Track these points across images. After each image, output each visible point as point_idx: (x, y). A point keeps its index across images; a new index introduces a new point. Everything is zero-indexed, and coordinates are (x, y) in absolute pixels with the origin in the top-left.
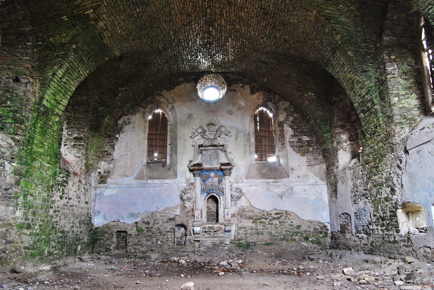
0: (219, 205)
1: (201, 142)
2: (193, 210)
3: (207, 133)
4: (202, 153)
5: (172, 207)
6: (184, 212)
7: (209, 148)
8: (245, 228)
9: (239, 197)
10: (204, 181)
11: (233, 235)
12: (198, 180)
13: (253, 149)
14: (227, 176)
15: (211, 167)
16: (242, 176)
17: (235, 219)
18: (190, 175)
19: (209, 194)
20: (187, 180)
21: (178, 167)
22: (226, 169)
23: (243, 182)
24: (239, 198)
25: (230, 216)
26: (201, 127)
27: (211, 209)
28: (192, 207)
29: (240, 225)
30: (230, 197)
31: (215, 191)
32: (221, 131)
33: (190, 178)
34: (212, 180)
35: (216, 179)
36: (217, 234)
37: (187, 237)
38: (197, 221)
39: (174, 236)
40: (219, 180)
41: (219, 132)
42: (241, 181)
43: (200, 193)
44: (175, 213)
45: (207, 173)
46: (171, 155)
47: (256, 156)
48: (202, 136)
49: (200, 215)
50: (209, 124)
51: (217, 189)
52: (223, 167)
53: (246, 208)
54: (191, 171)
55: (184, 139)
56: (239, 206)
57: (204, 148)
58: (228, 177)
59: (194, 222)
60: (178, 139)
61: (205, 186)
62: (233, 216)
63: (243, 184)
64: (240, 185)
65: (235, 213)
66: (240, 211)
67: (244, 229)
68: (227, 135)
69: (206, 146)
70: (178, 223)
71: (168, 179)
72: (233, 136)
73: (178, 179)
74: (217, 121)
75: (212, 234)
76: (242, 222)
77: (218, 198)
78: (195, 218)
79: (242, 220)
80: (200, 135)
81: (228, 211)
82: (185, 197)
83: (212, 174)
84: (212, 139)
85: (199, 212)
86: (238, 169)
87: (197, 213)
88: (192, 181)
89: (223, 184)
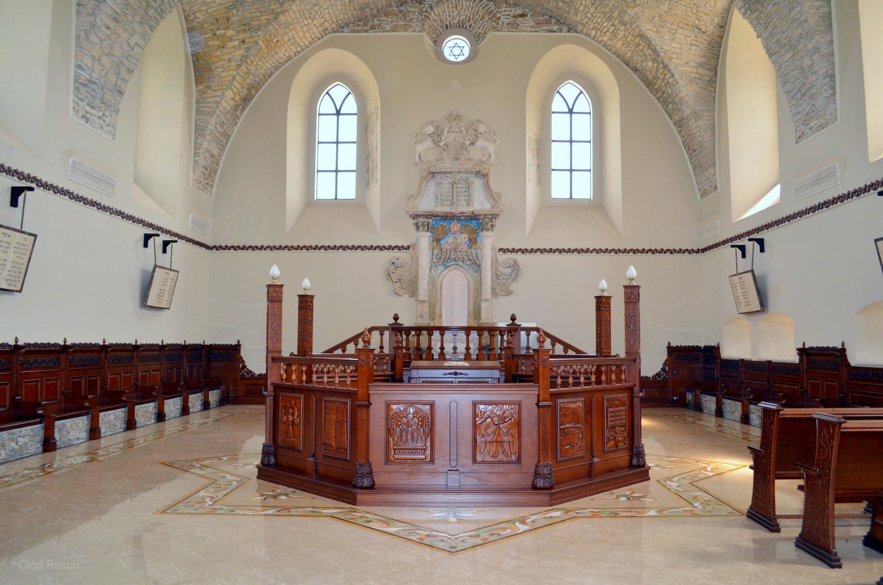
10: (437, 240)
14: (488, 230)
32: (476, 131)
34: (455, 238)
35: (463, 238)
40: (470, 240)
45: (445, 224)
51: (466, 258)
58: (490, 233)
80: (429, 140)
83: (455, 226)
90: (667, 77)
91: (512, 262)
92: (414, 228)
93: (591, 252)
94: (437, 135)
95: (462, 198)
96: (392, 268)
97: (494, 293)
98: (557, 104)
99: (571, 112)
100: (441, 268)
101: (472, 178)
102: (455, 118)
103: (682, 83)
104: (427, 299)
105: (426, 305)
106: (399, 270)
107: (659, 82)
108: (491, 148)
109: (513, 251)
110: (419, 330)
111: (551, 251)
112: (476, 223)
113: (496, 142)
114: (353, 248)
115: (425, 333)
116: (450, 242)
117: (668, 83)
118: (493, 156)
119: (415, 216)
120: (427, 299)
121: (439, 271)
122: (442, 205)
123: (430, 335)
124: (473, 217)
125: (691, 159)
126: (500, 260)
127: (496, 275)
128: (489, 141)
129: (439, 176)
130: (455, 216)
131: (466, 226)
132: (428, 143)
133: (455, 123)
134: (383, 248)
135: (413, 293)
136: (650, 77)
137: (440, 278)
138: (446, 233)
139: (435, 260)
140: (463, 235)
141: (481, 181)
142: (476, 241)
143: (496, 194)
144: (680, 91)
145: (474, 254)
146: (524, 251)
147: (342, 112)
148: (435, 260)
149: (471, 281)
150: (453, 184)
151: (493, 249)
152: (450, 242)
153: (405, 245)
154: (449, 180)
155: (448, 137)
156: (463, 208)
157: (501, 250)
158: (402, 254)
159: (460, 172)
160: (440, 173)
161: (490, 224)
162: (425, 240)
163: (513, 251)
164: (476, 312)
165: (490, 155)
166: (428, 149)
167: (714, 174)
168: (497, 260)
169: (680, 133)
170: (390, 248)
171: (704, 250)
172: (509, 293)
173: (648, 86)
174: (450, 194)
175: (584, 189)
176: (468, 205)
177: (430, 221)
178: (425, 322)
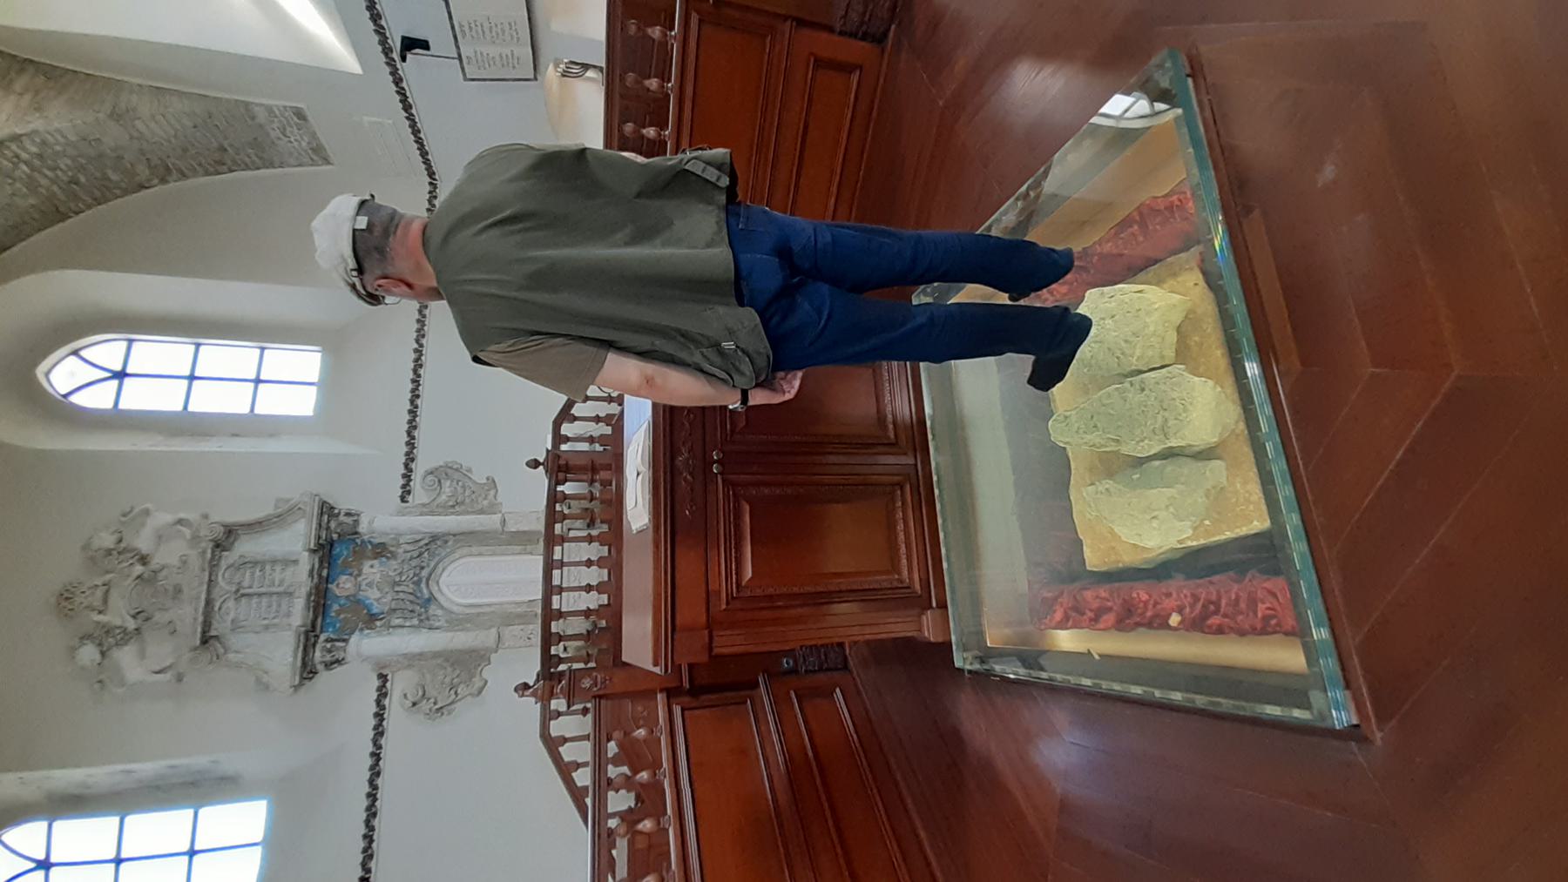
10: (371, 620)
14: (356, 522)
32: (109, 552)
34: (370, 585)
35: (372, 570)
40: (377, 555)
45: (336, 607)
51: (414, 563)
61: (399, 613)
90: (24, 156)
91: (430, 477)
92: (338, 670)
93: (421, 346)
94: (108, 639)
95: (277, 576)
96: (425, 706)
97: (492, 509)
98: (98, 398)
99: (121, 375)
100: (433, 610)
101: (229, 558)
102: (65, 600)
103: (36, 123)
104: (494, 631)
105: (507, 632)
106: (431, 692)
107: (44, 182)
108: (163, 518)
109: (407, 477)
110: (548, 639)
111: (413, 412)
112: (337, 543)
113: (147, 512)
114: (372, 796)
115: (555, 627)
116: (378, 595)
117: (40, 156)
118: (182, 515)
119: (308, 671)
120: (494, 631)
121: (439, 612)
122: (288, 615)
123: (561, 615)
124: (325, 550)
125: (247, 168)
126: (426, 500)
127: (454, 507)
128: (143, 525)
129: (215, 624)
130: (317, 587)
131: (346, 565)
132: (125, 656)
133: (78, 600)
134: (379, 732)
135: (482, 657)
136: (32, 201)
137: (455, 609)
138: (356, 603)
139: (415, 621)
140: (366, 569)
141: (243, 538)
143: (276, 507)
144: (58, 131)
145: (409, 548)
146: (410, 458)
147: (42, 856)
148: (415, 621)
149: (465, 550)
150: (240, 595)
151: (401, 513)
152: (378, 595)
153: (376, 683)
154: (231, 604)
155: (118, 615)
156: (300, 577)
157: (403, 499)
158: (397, 687)
159: (211, 582)
160: (207, 624)
162: (367, 645)
163: (407, 477)
164: (520, 539)
165: (180, 522)
166: (142, 655)
167: (269, 109)
168: (424, 505)
169: (184, 176)
170: (379, 716)
171: (431, 174)
172: (492, 483)
173: (63, 217)
174: (265, 600)
175: (305, 363)
176: (296, 562)
177: (323, 637)
178: (537, 628)
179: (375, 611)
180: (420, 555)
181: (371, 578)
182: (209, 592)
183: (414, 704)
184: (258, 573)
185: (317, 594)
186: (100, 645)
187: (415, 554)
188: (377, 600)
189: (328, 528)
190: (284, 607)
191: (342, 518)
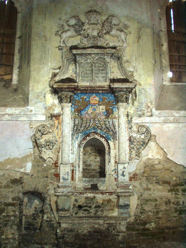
0: (107, 156)
1: (76, 41)
2: (56, 164)
3: (86, 27)
4: (75, 61)
5: (18, 159)
6: (40, 169)
7: (89, 51)
8: (156, 200)
9: (144, 143)
11: (132, 214)
12: (68, 110)
13: (166, 62)
15: (92, 84)
16: (149, 104)
17: (137, 183)
18: (52, 100)
19: (88, 135)
20: (47, 109)
21: (31, 85)
22: (121, 90)
23: (151, 116)
24: (145, 144)
25: (127, 178)
26: (76, 17)
27: (90, 165)
28: (55, 159)
29: (146, 195)
30: (128, 143)
31: (99, 131)
32: (111, 23)
33: (54, 105)
34: (95, 109)
35: (102, 109)
36: (102, 210)
37: (45, 216)
38: (65, 187)
39: (21, 212)
40: (107, 111)
41: (106, 24)
42: (149, 114)
43: (71, 133)
44: (22, 170)
45: (85, 97)
46: (20, 67)
47: (170, 74)
48: (76, 31)
49: (70, 174)
50: (90, 11)
51: (103, 126)
52: (116, 85)
53: (156, 162)
54: (55, 91)
55: (45, 36)
56: (144, 159)
57: (79, 52)
58: (125, 104)
59: (59, 187)
60: (33, 36)
62: (134, 177)
63: (152, 119)
64: (146, 120)
65: (138, 172)
66: (147, 169)
67: (153, 203)
68: (121, 31)
69: (84, 48)
70: (28, 188)
71: (11, 106)
72: (132, 32)
73: (30, 108)
74: (104, 8)
75: (93, 211)
76: (149, 189)
77: (105, 143)
78: (61, 180)
79: (150, 186)
80: (72, 30)
81: (124, 168)
82: (42, 141)
83: (94, 99)
84: (94, 37)
85: (68, 169)
86: (143, 91)
87: (64, 171)
88: (57, 111)
89: (115, 118)
116: (90, 112)
138: (87, 104)
140: (102, 107)
142: (112, 112)
145: (111, 123)
152: (90, 112)
161: (124, 96)
179: (82, 112)
180: (107, 128)
181: (98, 109)
182: (94, 54)
183: (40, 131)
184: (101, 69)
185: (91, 90)
186: (76, 25)
187: (108, 126)
188: (87, 113)
189: (120, 91)
190: (86, 79)
191: (124, 96)
